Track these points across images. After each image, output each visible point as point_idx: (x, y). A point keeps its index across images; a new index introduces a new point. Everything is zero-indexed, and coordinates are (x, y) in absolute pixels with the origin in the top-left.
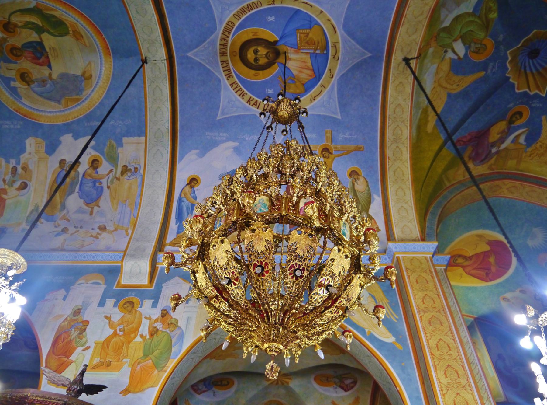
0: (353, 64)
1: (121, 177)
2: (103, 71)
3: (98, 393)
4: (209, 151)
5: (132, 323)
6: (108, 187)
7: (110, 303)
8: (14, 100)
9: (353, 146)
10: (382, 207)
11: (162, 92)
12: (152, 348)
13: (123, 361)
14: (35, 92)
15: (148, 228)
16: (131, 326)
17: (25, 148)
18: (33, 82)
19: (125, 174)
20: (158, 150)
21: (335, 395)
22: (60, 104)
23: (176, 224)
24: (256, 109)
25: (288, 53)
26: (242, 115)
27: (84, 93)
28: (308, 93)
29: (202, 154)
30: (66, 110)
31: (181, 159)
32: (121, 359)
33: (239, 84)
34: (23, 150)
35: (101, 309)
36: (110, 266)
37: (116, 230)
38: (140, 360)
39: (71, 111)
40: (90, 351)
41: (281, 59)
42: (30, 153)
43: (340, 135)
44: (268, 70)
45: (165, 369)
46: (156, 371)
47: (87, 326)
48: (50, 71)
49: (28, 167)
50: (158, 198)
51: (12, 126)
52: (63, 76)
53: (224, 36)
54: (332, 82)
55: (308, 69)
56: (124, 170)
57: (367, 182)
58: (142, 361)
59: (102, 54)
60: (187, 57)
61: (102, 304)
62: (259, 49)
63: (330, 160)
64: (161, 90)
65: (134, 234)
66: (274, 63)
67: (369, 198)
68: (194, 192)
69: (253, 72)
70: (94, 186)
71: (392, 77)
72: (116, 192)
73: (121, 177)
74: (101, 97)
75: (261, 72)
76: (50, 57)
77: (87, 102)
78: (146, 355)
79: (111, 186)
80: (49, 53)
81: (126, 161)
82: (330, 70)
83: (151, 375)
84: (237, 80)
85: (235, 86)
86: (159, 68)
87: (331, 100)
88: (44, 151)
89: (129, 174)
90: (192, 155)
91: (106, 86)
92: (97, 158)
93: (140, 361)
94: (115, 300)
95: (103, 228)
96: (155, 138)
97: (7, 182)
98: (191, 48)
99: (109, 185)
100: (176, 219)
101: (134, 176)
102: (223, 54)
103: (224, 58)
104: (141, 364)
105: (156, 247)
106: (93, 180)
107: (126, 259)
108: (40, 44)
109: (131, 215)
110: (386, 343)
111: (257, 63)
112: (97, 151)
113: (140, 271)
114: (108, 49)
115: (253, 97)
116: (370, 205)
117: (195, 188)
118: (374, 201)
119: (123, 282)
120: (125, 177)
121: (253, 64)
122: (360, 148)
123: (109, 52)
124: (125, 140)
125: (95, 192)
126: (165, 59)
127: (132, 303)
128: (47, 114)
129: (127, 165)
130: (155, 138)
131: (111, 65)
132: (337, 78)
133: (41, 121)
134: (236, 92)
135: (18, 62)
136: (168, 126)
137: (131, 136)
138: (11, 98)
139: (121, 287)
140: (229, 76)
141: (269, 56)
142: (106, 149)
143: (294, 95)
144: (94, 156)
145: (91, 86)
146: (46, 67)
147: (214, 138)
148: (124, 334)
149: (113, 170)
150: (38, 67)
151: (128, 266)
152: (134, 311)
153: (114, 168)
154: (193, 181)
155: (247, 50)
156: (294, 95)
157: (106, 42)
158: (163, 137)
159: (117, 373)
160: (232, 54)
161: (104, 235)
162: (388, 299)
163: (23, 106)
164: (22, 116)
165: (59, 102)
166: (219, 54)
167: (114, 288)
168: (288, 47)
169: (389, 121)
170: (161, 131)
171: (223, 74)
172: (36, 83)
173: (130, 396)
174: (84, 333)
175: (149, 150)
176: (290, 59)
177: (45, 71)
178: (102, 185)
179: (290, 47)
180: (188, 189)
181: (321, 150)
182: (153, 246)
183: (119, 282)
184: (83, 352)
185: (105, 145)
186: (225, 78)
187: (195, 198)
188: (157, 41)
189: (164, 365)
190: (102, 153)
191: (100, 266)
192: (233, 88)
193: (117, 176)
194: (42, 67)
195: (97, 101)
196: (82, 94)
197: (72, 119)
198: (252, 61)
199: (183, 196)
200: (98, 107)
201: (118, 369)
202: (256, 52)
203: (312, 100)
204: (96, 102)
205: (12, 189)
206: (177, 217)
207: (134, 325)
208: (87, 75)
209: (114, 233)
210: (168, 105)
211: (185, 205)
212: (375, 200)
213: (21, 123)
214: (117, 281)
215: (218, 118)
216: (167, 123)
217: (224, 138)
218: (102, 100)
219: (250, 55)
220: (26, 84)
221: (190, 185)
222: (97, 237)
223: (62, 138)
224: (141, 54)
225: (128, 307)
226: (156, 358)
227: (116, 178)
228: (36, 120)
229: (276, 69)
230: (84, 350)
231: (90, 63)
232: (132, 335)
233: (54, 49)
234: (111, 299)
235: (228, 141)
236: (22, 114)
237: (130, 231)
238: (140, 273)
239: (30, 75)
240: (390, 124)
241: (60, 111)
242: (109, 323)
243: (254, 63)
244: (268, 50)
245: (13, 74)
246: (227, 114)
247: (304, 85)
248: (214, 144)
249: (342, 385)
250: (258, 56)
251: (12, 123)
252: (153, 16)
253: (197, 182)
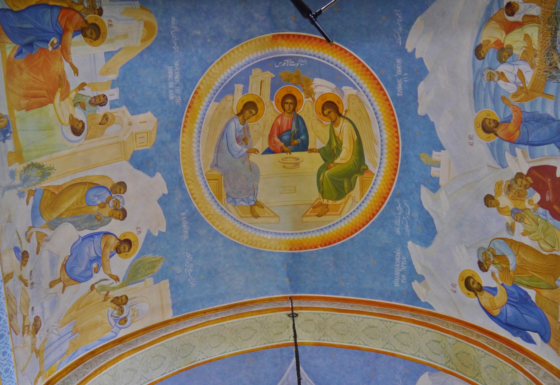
1: (110, 300)
2: (266, 235)
6: (92, 287)
8: (214, 88)
11: (247, 340)
14: (227, 125)
17: (139, 113)
18: (243, 122)
19: (114, 306)
20: (165, 358)
22: (212, 167)
27: (230, 206)
30: (203, 178)
34: (135, 109)
39: (203, 187)
42: (130, 124)
48: (261, 152)
49: (109, 125)
51: (171, 85)
52: (253, 169)
59: (292, 237)
64: (250, 338)
70: (92, 261)
72: (88, 304)
74: (226, 233)
76: (284, 155)
77: (218, 211)
80: (288, 155)
81: (135, 297)
86: (281, 333)
88: (136, 149)
89: (116, 312)
91: (243, 241)
92: (133, 246)
96: (182, 346)
97: (81, 92)
99: (96, 286)
101: (113, 323)
106: (100, 255)
108: (304, 147)
112: (144, 244)
114: (301, 249)
123: (296, 249)
124: (165, 284)
125: (83, 268)
128: (195, 145)
129: (129, 302)
130: (182, 346)
131: (275, 249)
133: (183, 137)
135: (274, 102)
136: (199, 360)
137: (172, 293)
138: (217, 84)
142: (150, 257)
144: (137, 240)
145: (241, 217)
146: (266, 146)
149: (119, 280)
150: (267, 133)
157: (311, 248)
158: (182, 358)
163: (204, 104)
164: (189, 103)
165: (215, 165)
170: (192, 352)
172: (241, 127)
177: (261, 144)
178: (95, 275)
185: (155, 252)
190: (142, 253)
193: (110, 293)
194: (266, 139)
195: (220, 227)
196: (229, 202)
197: (190, 190)
200: (210, 230)
204: (217, 226)
205: (71, 107)
208: (257, 209)
210: (230, 351)
213: (178, 101)
216: (203, 356)
218: (222, 236)
220: (239, 111)
223: (159, 176)
227: (107, 295)
228: (185, 127)
231: (276, 216)
233: (297, 164)
236: (192, 102)
239: (254, 117)
241: (201, 169)
245: (254, 89)
251: (177, 85)
252: (364, 344)
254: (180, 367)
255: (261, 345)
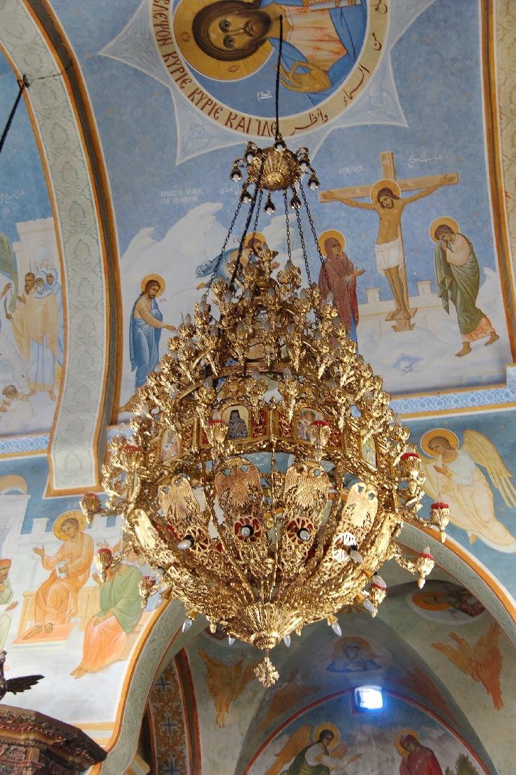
0: (419, 14)
1: (26, 296)
3: (30, 688)
4: (172, 225)
5: (78, 558)
7: (39, 524)
9: (438, 177)
10: (500, 290)
12: (114, 595)
13: (71, 622)
15: (84, 385)
16: (77, 562)
20: (81, 240)
21: (454, 623)
23: (133, 370)
24: (245, 135)
25: (286, 17)
26: (221, 150)
28: (337, 88)
29: (159, 235)
31: (125, 248)
32: (67, 619)
33: (206, 93)
35: (26, 538)
36: (32, 459)
37: (33, 392)
38: (96, 617)
40: (19, 609)
41: (274, 32)
43: (410, 159)
44: (255, 55)
45: (136, 629)
46: (124, 633)
47: (9, 568)
50: (94, 329)
53: (158, 8)
54: (381, 56)
55: (331, 40)
56: (30, 283)
57: (469, 244)
58: (100, 619)
60: (100, 57)
61: (27, 528)
62: (229, 19)
63: (395, 211)
64: (65, 130)
65: (62, 400)
66: (263, 41)
67: (474, 276)
68: (156, 307)
69: (226, 65)
71: (498, 30)
72: (22, 324)
73: (26, 296)
75: (240, 63)
78: (105, 610)
79: (13, 314)
81: (30, 265)
82: (374, 35)
83: (115, 642)
84: (200, 86)
85: (197, 97)
86: (53, 91)
87: (384, 94)
89: (39, 288)
90: (143, 238)
93: (97, 619)
94: (48, 519)
95: (11, 392)
96: (71, 219)
98: (98, 49)
99: (9, 312)
100: (131, 360)
101: (49, 291)
102: (164, 40)
103: (168, 49)
104: (100, 625)
105: (101, 419)
107: (54, 448)
109: (54, 362)
110: (504, 554)
111: (231, 46)
113: (81, 465)
115: (235, 111)
116: (477, 289)
117: (157, 299)
118: (485, 280)
119: (56, 487)
120: (34, 293)
121: (222, 50)
122: (451, 179)
124: (20, 226)
126: (60, 72)
127: (74, 522)
132: (391, 48)
134: (202, 109)
136: (90, 195)
137: (30, 219)
139: (53, 495)
140: (183, 80)
141: (252, 29)
143: (312, 96)
147: (176, 200)
148: (68, 575)
149: (10, 284)
151: (58, 459)
152: (79, 534)
153: (11, 281)
154: (151, 287)
155: (208, 25)
156: (312, 96)
159: (63, 643)
160: (182, 38)
161: (15, 404)
162: (510, 472)
166: (156, 43)
167: (44, 498)
168: (283, 7)
169: (501, 119)
171: (172, 78)
173: (86, 678)
174: (5, 581)
175: (64, 243)
176: (292, 28)
179: (286, 5)
180: (144, 302)
181: (376, 193)
182: (96, 419)
183: (49, 487)
184: (8, 612)
186: (177, 85)
187: (160, 318)
188: (37, 44)
189: (134, 623)
191: (16, 461)
192: (195, 101)
193: (20, 295)
198: (220, 44)
199: (138, 316)
201: (64, 634)
202: (224, 27)
203: (347, 99)
206: (133, 357)
207: (83, 560)
209: (31, 398)
210: (82, 155)
211: (143, 332)
212: (487, 278)
214: (47, 485)
215: (178, 163)
217: (196, 199)
219: (215, 35)
221: (147, 295)
222: (4, 411)
224: (16, 72)
225: (69, 529)
226: (121, 612)
227: (20, 298)
229: (268, 52)
230: (7, 610)
232: (81, 578)
234: (40, 517)
235: (203, 203)
237: (56, 393)
238: (81, 468)
240: (503, 126)
242: (43, 559)
243: (224, 48)
244: (248, 19)
246: (193, 153)
247: (326, 72)
248: (180, 212)
249: (463, 606)
250: (229, 34)
253: (159, 286)
254: (95, 220)
255: (72, 116)
